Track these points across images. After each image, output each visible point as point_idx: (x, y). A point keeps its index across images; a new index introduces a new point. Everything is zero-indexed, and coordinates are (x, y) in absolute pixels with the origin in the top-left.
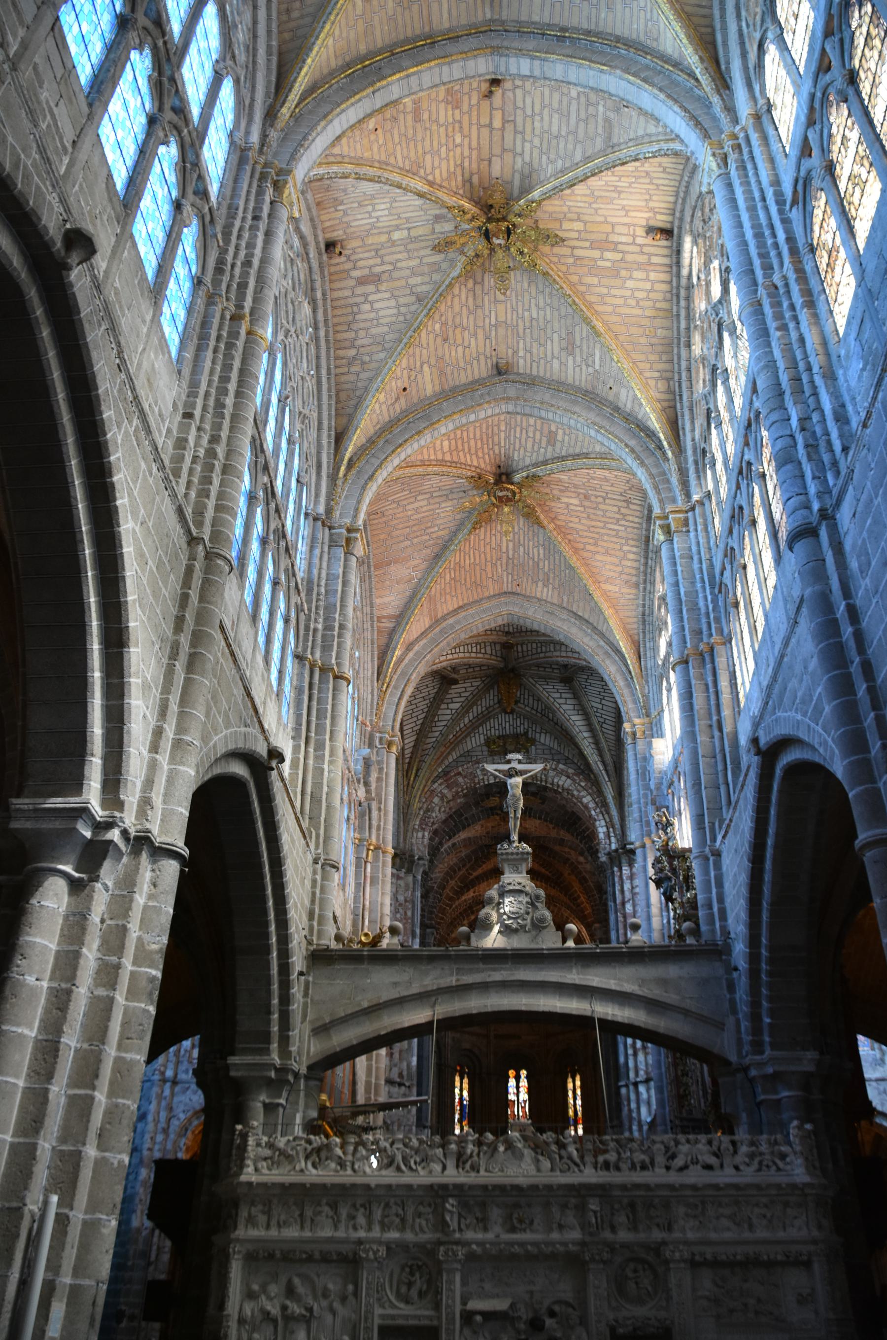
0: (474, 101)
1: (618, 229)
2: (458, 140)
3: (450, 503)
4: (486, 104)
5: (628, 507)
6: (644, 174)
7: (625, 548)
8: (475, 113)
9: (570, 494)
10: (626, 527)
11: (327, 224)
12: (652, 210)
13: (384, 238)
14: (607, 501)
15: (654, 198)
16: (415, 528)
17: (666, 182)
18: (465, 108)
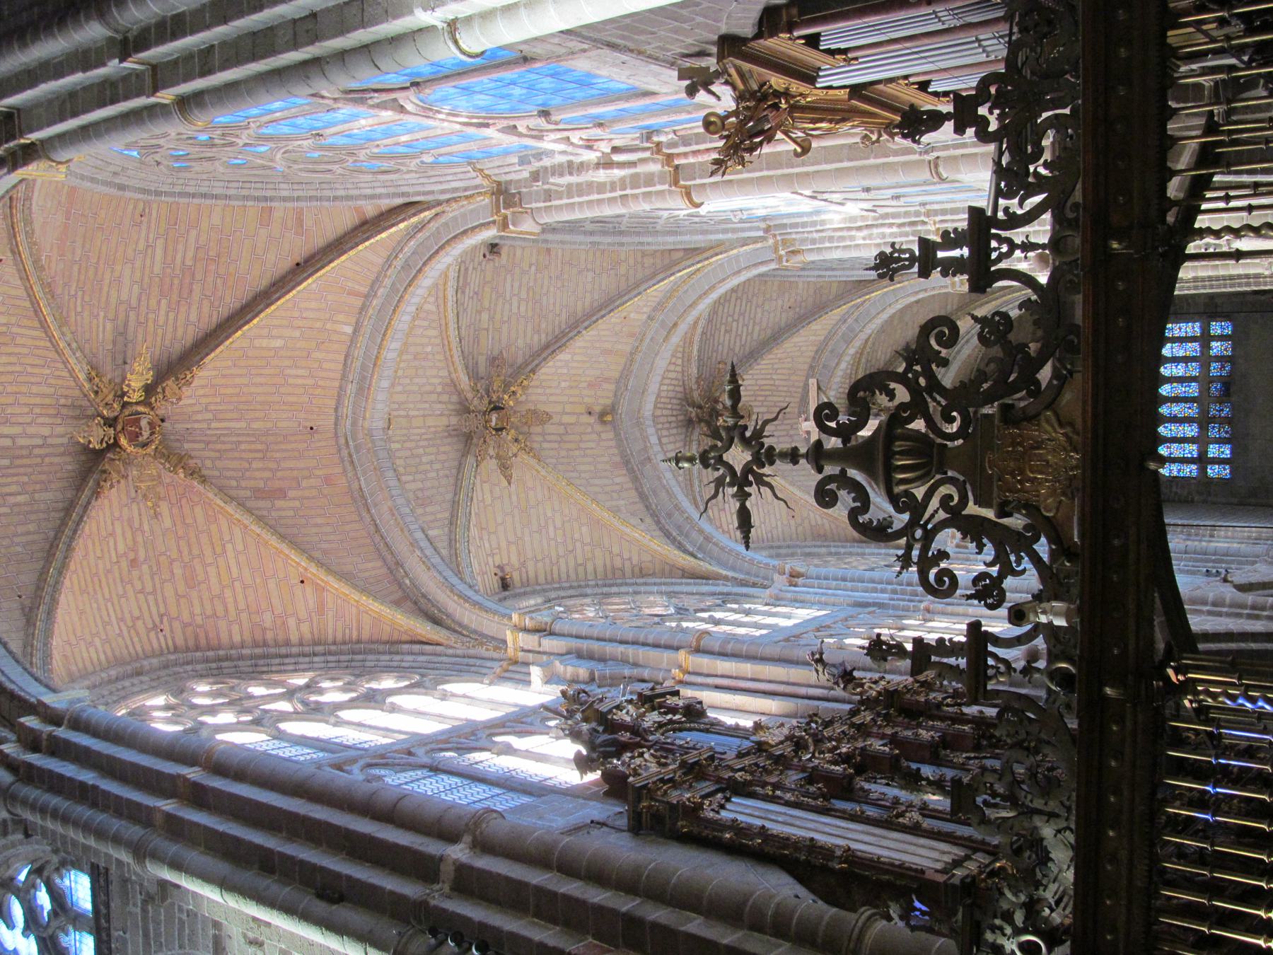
0: (586, 400)
1: (493, 537)
2: (563, 384)
3: (109, 336)
4: (582, 409)
5: (149, 631)
6: (570, 548)
7: (97, 642)
8: (576, 399)
9: (129, 535)
10: (121, 635)
11: (519, 252)
12: (523, 564)
13: (486, 304)
14: (141, 596)
15: (540, 565)
16: (91, 273)
17: (563, 569)
18: (585, 392)
